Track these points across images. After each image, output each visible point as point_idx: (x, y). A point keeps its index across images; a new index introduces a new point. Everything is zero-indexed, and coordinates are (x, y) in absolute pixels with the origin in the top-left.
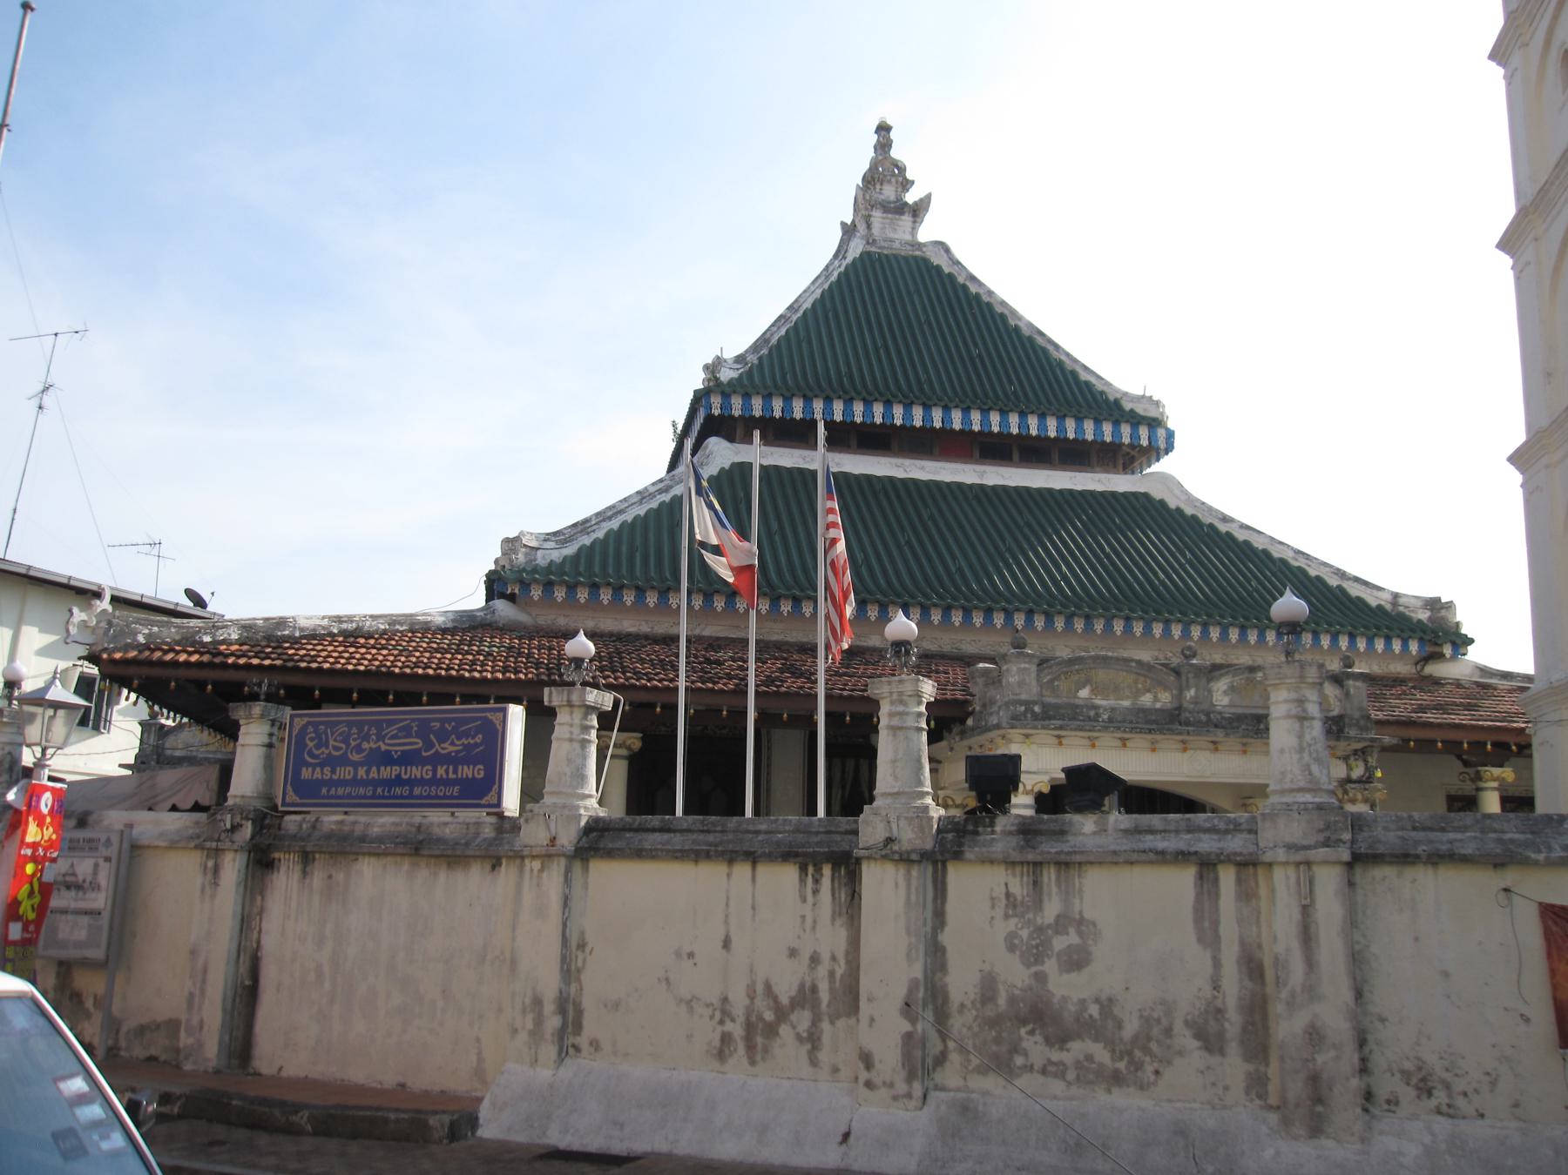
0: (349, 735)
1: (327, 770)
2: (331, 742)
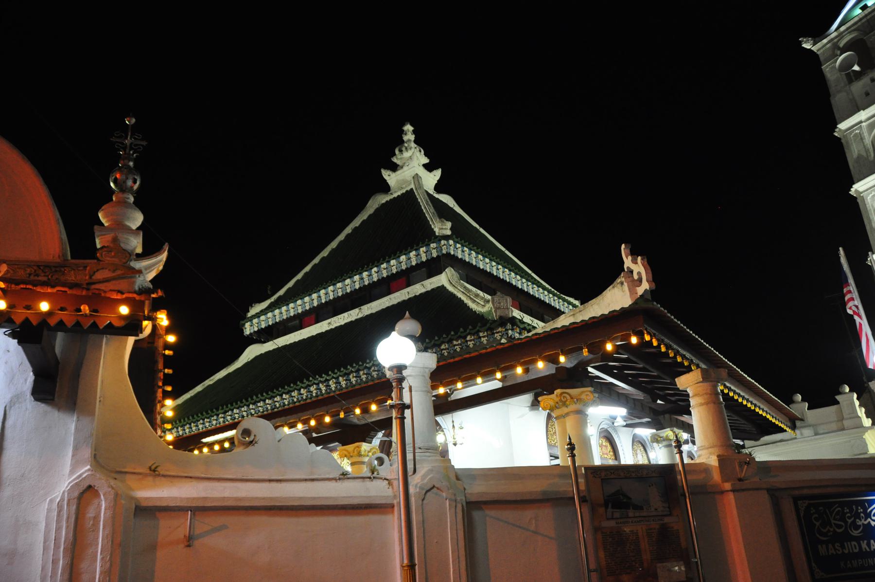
1: (837, 545)
2: (833, 521)
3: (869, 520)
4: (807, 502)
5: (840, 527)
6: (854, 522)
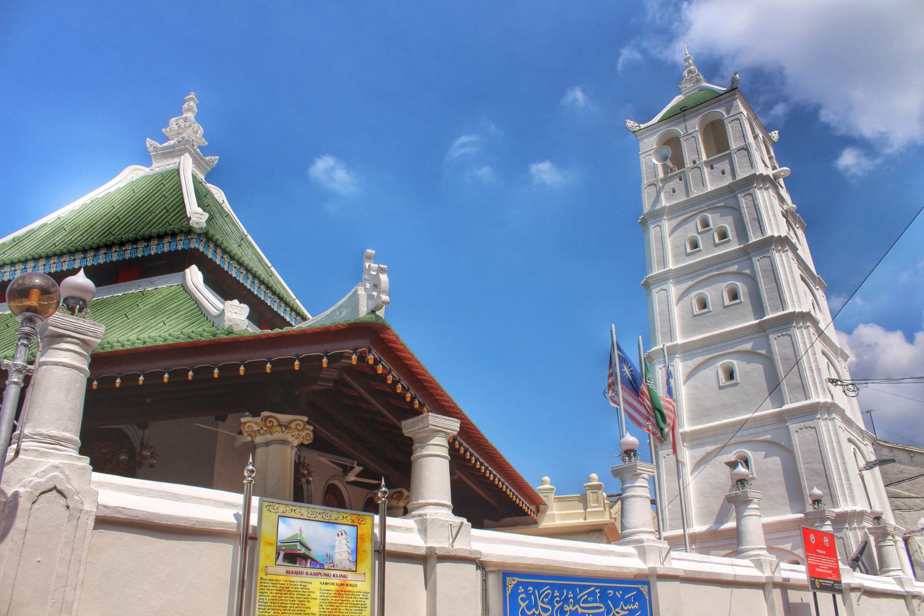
0: (553, 597)
2: (540, 604)
3: (577, 606)
4: (517, 579)
5: (545, 610)
6: (562, 606)
